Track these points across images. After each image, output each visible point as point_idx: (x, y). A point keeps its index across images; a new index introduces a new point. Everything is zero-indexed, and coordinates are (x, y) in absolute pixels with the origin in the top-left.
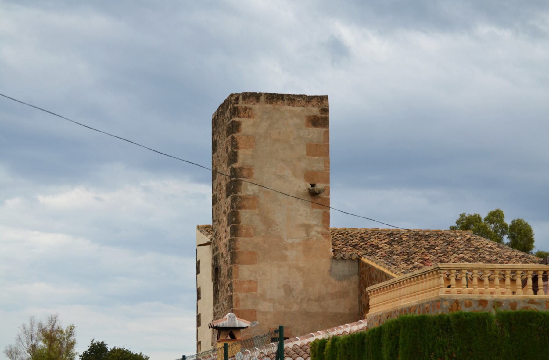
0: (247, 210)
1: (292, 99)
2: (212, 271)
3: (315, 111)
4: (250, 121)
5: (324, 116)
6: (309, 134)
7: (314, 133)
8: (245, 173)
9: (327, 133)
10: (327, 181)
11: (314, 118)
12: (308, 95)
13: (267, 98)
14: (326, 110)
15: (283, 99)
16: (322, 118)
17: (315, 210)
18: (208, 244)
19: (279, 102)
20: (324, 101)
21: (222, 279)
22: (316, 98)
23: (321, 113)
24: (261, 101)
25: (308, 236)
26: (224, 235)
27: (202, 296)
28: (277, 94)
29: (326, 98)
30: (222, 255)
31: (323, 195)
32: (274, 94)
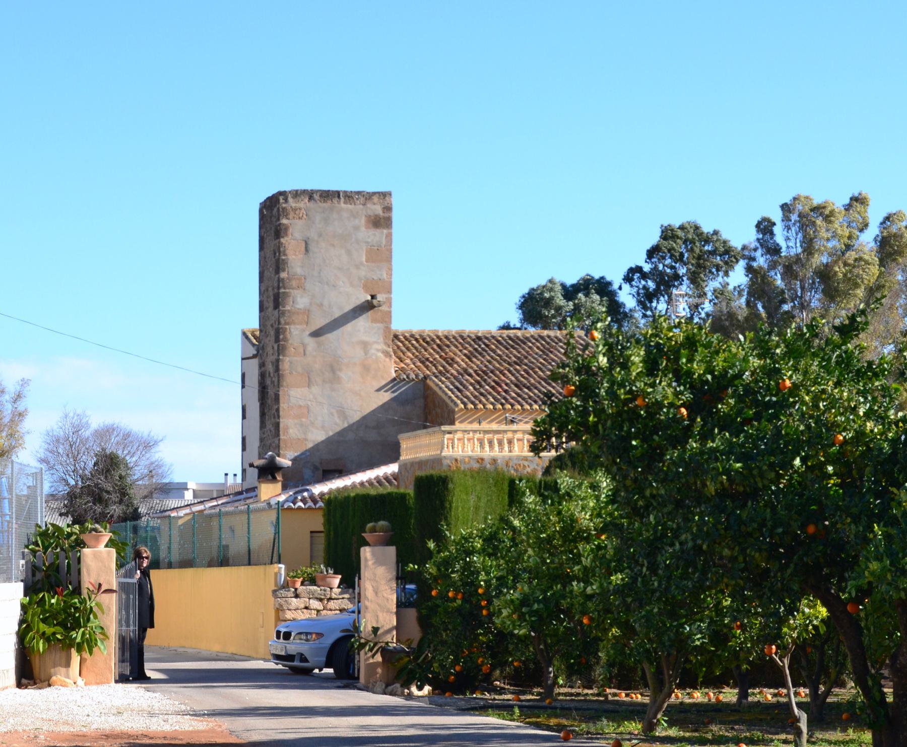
0: (298, 326)
1: (349, 196)
2: (259, 390)
3: (378, 209)
4: (299, 223)
5: (386, 215)
6: (369, 237)
7: (376, 236)
8: (294, 283)
9: (389, 237)
10: (389, 291)
11: (375, 219)
12: (368, 191)
13: (321, 196)
14: (388, 209)
15: (339, 197)
16: (384, 218)
17: (375, 325)
18: (254, 356)
19: (335, 200)
20: (387, 198)
21: (269, 401)
22: (377, 195)
23: (384, 212)
24: (342, 413)
25: (366, 355)
26: (271, 352)
27: (247, 416)
28: (332, 191)
29: (390, 194)
30: (269, 374)
31: (384, 308)
32: (329, 191)
